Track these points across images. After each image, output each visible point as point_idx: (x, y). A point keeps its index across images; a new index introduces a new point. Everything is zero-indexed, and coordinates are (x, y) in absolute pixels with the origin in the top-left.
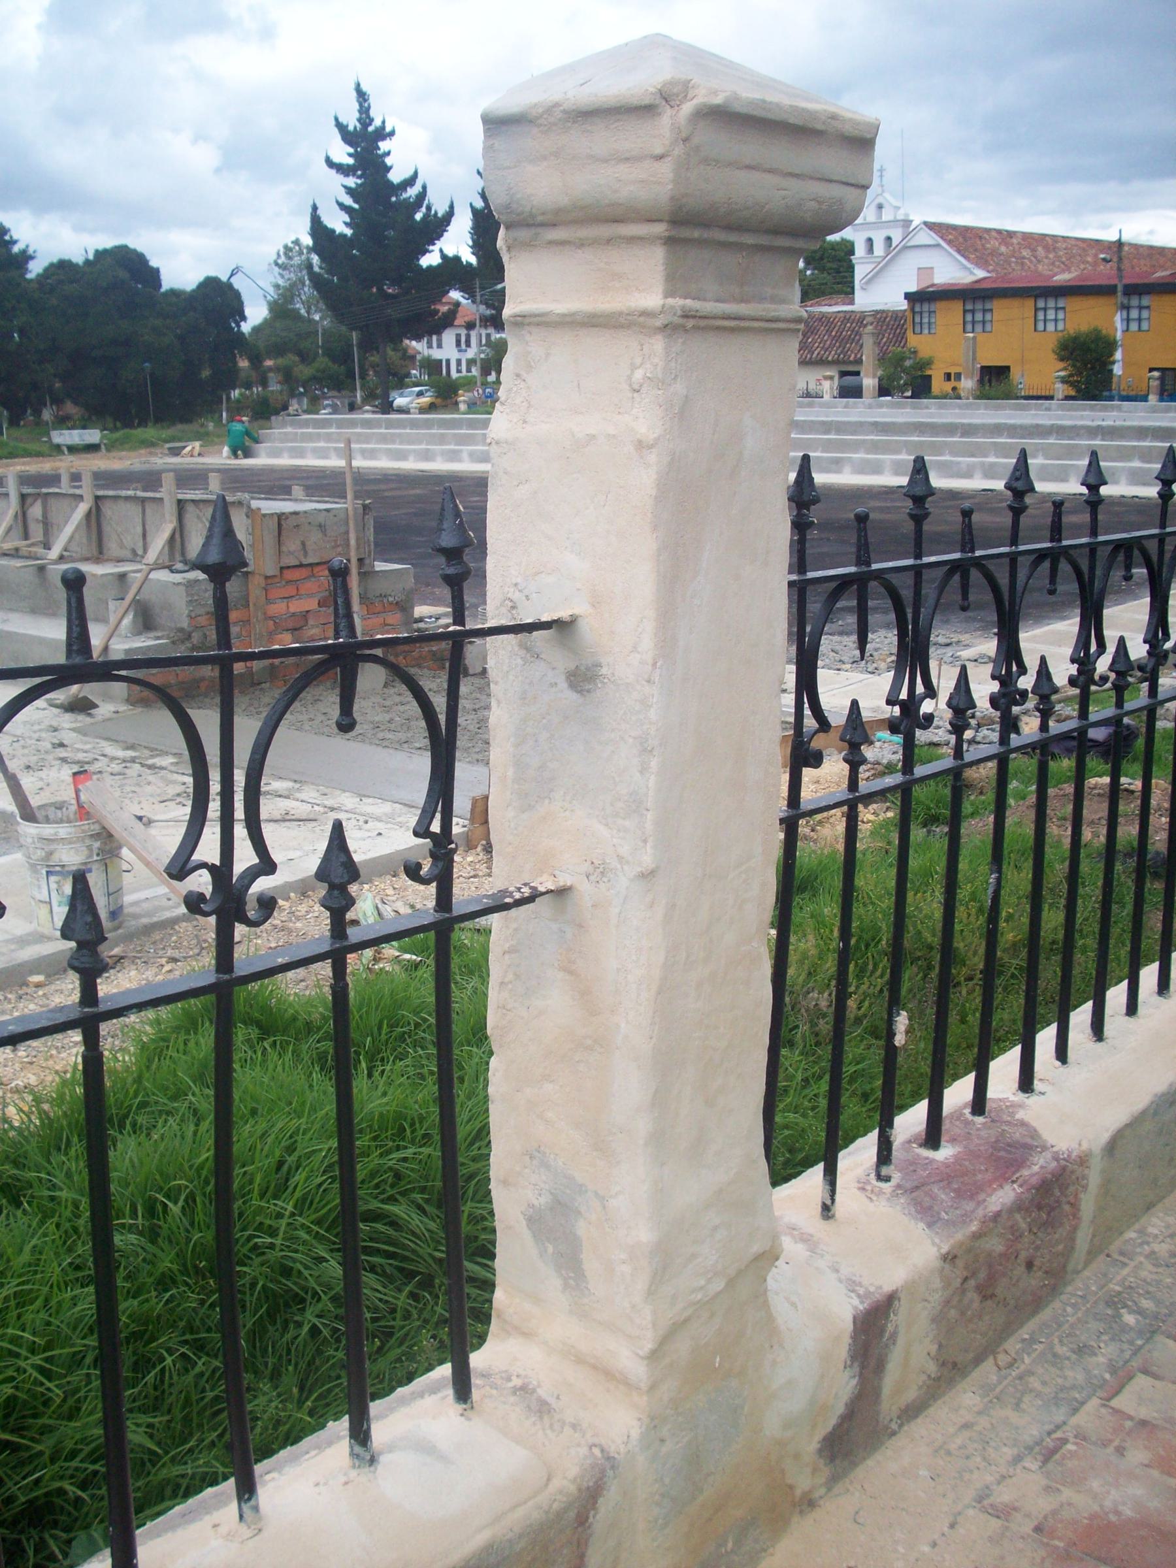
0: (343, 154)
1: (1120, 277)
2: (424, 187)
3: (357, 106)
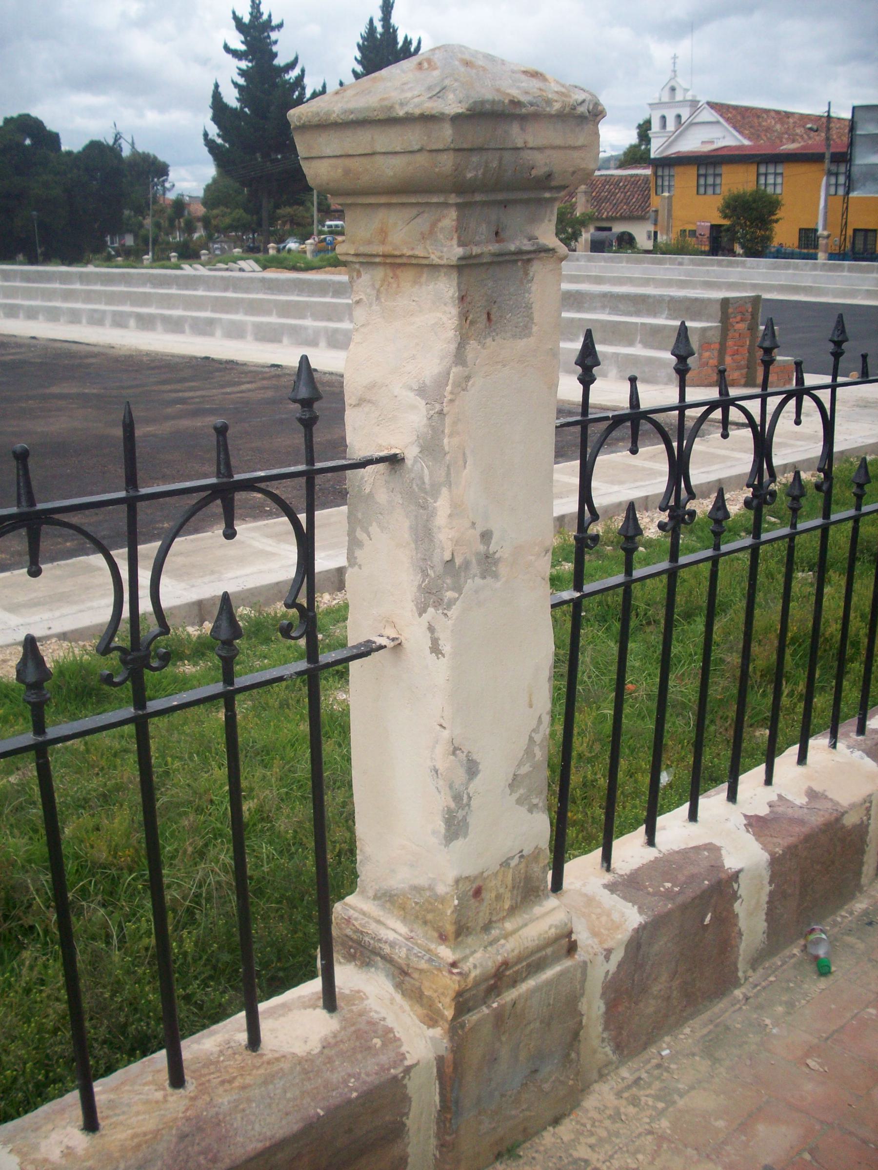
0: (237, 42)
1: (828, 146)
2: (303, 71)
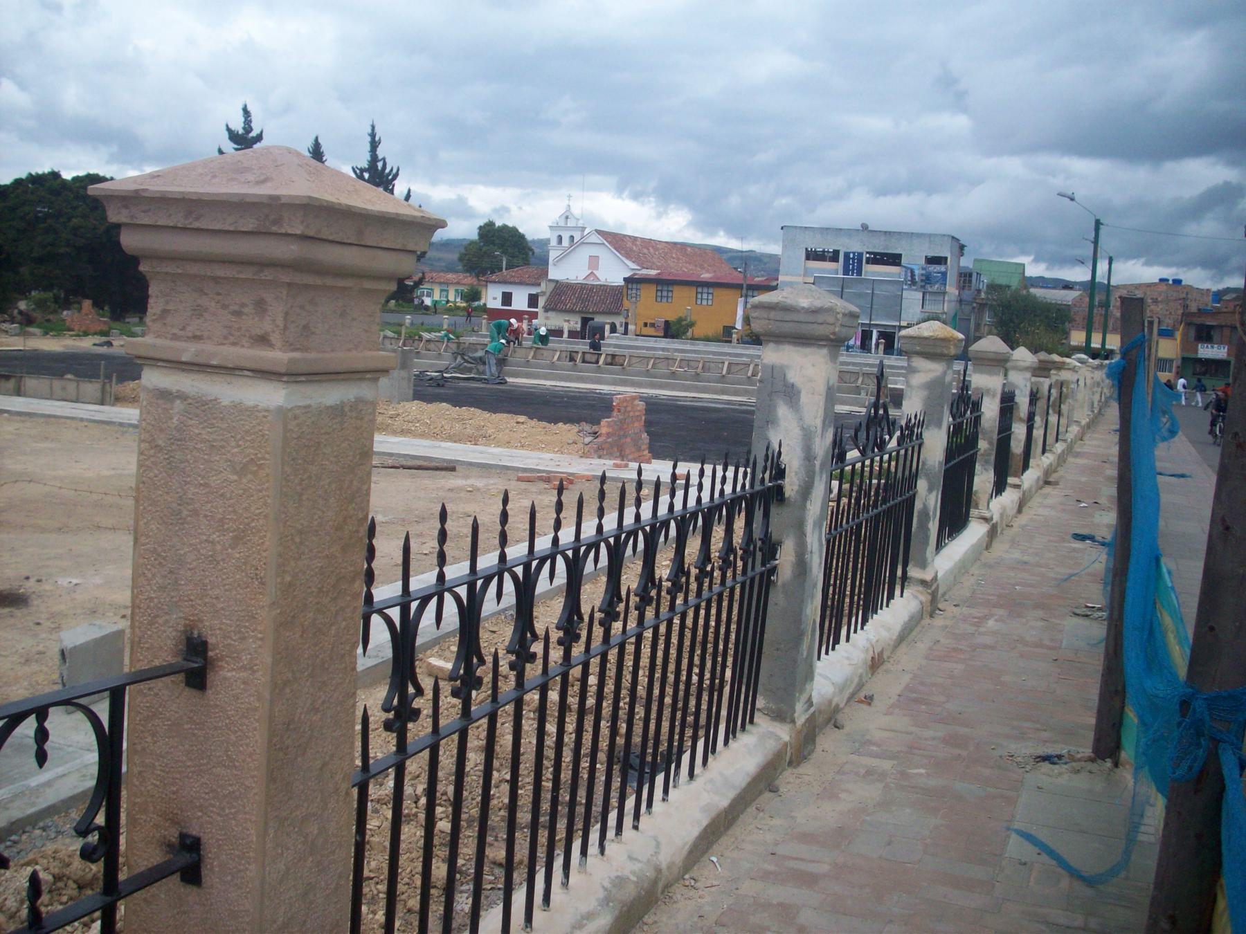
3: (243, 119)
